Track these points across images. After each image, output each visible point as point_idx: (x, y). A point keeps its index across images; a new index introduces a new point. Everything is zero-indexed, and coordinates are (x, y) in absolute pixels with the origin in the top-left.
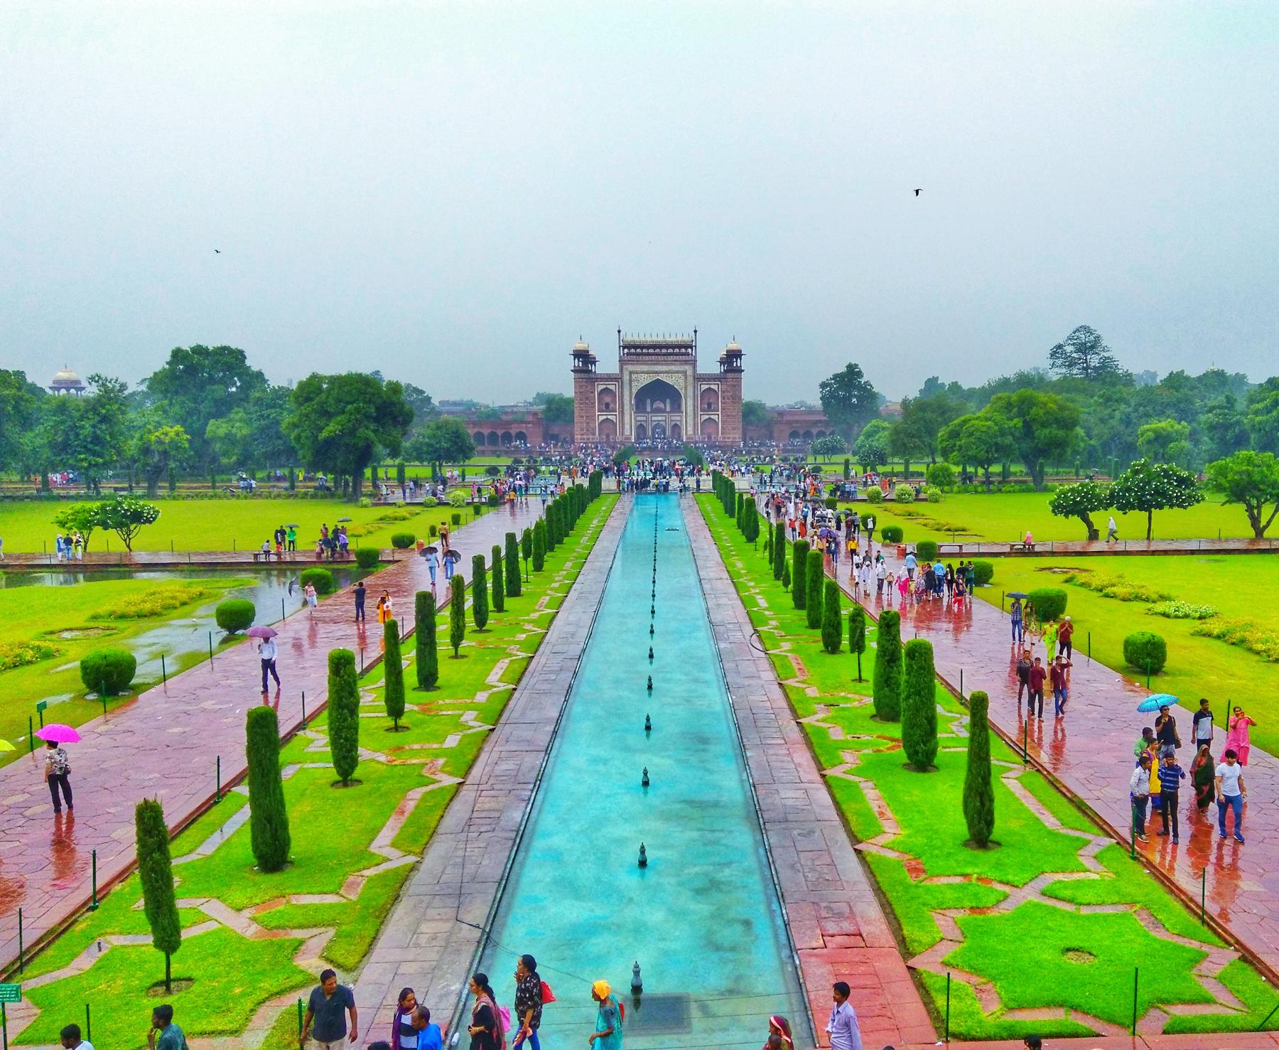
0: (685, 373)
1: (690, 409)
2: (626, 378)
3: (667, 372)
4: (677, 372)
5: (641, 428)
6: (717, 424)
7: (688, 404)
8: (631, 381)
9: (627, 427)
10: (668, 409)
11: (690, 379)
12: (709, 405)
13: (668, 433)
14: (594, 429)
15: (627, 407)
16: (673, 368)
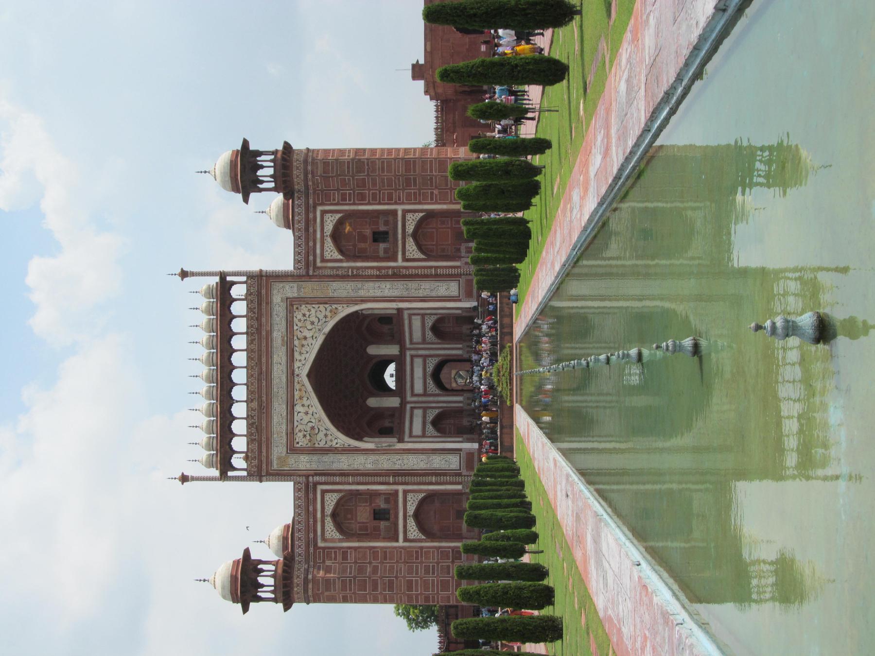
0: (292, 304)
1: (387, 288)
2: (304, 462)
3: (291, 358)
4: (290, 324)
5: (444, 423)
6: (430, 216)
7: (377, 296)
8: (313, 451)
9: (438, 462)
10: (393, 350)
11: (309, 289)
12: (379, 237)
13: (455, 350)
14: (443, 553)
15: (386, 463)
16: (278, 334)
